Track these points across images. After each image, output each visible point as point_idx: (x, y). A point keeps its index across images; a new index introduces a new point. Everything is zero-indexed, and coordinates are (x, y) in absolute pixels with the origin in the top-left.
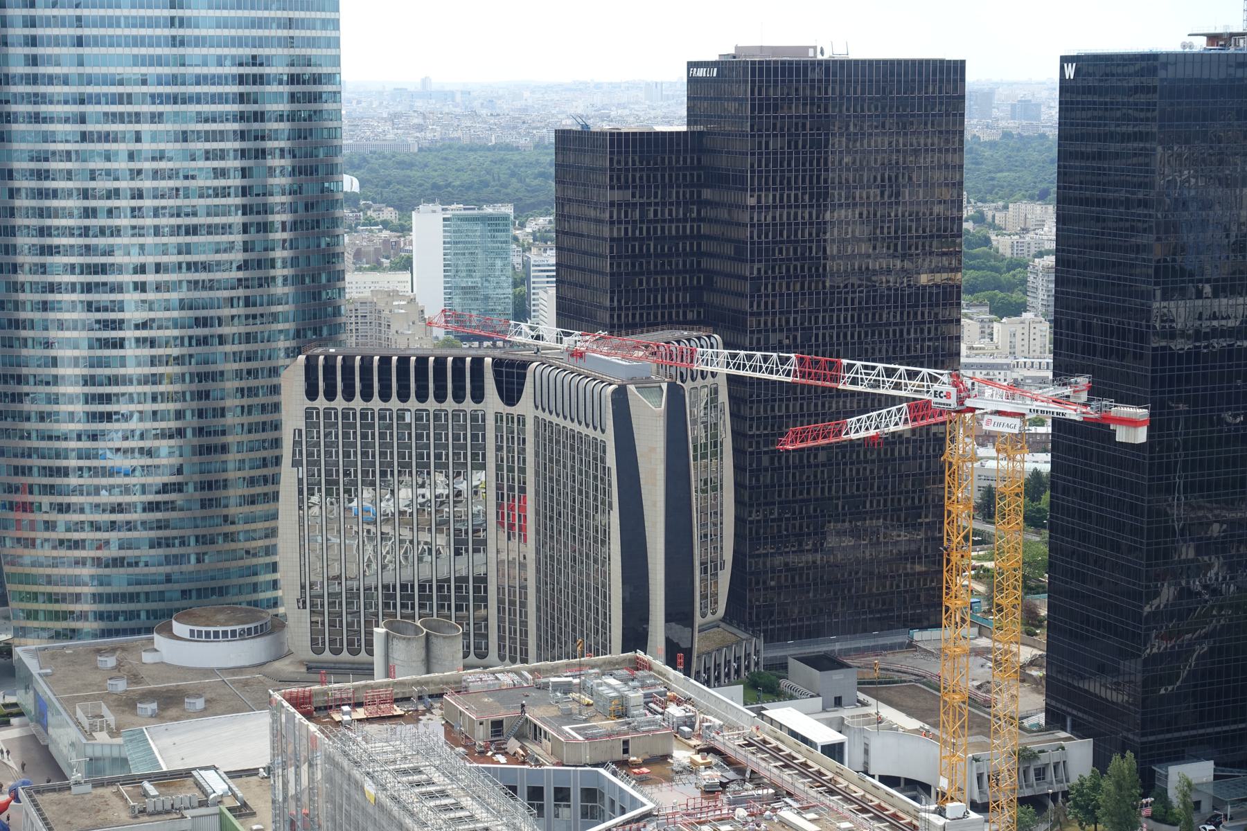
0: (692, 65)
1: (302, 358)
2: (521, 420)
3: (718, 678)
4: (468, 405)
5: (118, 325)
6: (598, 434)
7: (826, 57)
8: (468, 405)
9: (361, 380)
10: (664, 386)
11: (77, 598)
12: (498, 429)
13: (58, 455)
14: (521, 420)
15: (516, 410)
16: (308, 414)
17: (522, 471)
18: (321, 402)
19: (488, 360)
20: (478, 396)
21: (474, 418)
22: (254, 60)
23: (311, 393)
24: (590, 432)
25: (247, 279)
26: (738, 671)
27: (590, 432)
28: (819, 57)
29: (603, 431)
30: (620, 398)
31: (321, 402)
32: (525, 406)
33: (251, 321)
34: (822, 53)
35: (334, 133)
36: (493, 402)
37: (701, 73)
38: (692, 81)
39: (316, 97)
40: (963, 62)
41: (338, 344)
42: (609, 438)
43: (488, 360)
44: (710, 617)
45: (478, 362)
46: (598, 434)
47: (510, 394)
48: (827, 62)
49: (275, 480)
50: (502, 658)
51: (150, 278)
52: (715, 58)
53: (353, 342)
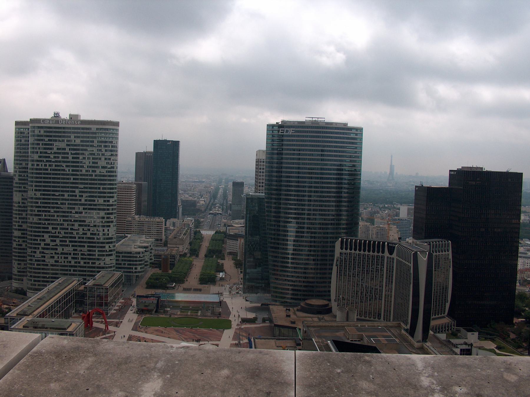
0: (450, 171)
1: (340, 239)
2: (393, 259)
3: (442, 331)
4: (380, 254)
5: (303, 228)
6: (409, 264)
7: (485, 170)
8: (380, 254)
9: (354, 246)
10: (427, 253)
11: (287, 294)
12: (387, 261)
13: (284, 258)
14: (393, 259)
15: (392, 256)
16: (341, 253)
17: (393, 272)
18: (344, 251)
19: (386, 243)
20: (383, 252)
21: (382, 257)
22: (341, 165)
23: (342, 248)
24: (408, 263)
25: (333, 219)
26: (448, 330)
27: (408, 263)
28: (484, 170)
29: (410, 263)
30: (415, 255)
31: (344, 251)
32: (394, 255)
33: (337, 229)
34: (484, 169)
35: (360, 183)
36: (387, 254)
37: (452, 173)
38: (450, 174)
39: (354, 175)
40: (521, 174)
41: (357, 236)
42: (412, 265)
43: (386, 243)
44: (443, 315)
45: (384, 243)
46: (409, 264)
47: (391, 253)
48: (485, 171)
49: (332, 269)
50: (384, 320)
51: (311, 217)
52: (456, 169)
53: (361, 235)
